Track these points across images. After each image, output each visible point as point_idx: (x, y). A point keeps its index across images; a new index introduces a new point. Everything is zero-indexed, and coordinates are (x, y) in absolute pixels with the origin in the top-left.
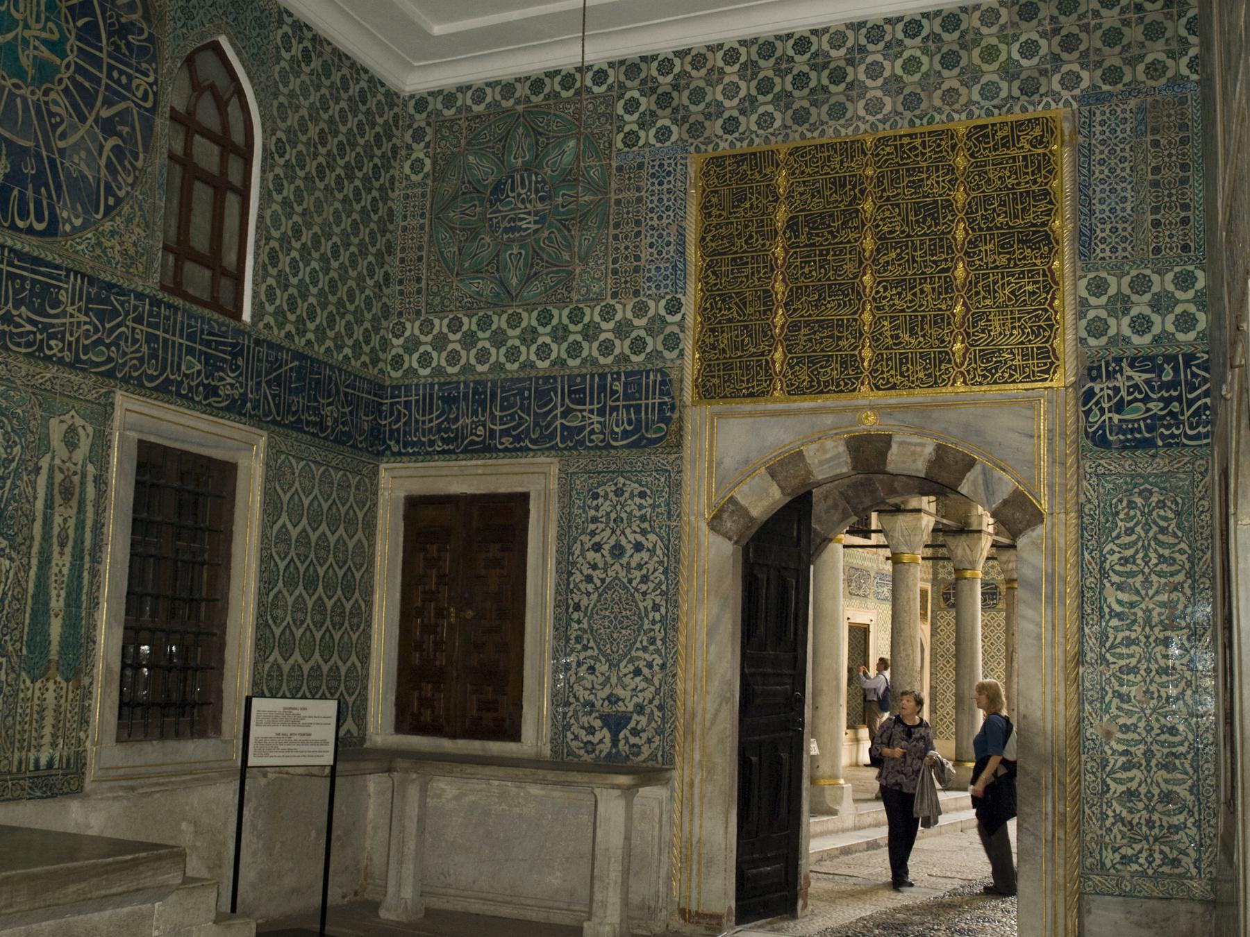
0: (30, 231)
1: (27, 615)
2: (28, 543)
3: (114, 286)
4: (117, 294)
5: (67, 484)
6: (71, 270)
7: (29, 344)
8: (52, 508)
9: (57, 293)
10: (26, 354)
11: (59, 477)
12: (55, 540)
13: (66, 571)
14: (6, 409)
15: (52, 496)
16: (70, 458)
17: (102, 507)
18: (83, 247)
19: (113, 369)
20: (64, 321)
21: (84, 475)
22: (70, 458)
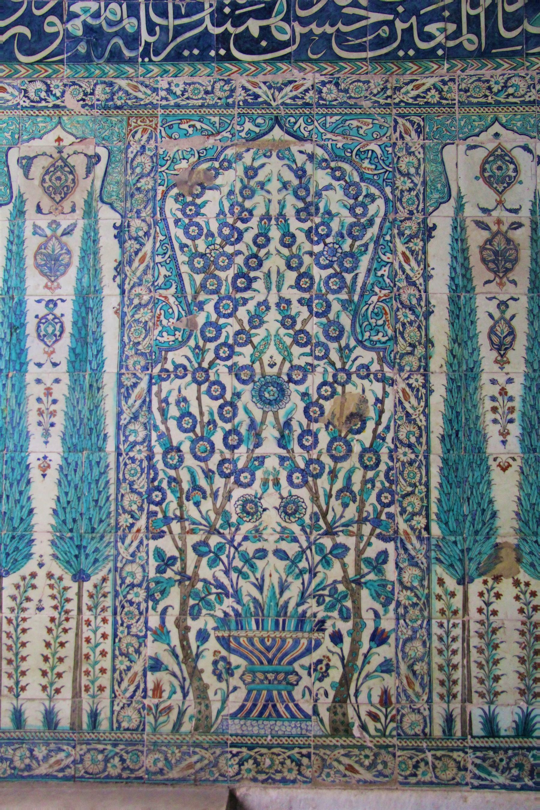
1: (434, 471)
2: (420, 351)
5: (499, 244)
7: (379, 43)
11: (476, 238)
12: (483, 340)
13: (516, 390)
14: (344, 148)
15: (467, 269)
16: (500, 203)
22: (500, 203)
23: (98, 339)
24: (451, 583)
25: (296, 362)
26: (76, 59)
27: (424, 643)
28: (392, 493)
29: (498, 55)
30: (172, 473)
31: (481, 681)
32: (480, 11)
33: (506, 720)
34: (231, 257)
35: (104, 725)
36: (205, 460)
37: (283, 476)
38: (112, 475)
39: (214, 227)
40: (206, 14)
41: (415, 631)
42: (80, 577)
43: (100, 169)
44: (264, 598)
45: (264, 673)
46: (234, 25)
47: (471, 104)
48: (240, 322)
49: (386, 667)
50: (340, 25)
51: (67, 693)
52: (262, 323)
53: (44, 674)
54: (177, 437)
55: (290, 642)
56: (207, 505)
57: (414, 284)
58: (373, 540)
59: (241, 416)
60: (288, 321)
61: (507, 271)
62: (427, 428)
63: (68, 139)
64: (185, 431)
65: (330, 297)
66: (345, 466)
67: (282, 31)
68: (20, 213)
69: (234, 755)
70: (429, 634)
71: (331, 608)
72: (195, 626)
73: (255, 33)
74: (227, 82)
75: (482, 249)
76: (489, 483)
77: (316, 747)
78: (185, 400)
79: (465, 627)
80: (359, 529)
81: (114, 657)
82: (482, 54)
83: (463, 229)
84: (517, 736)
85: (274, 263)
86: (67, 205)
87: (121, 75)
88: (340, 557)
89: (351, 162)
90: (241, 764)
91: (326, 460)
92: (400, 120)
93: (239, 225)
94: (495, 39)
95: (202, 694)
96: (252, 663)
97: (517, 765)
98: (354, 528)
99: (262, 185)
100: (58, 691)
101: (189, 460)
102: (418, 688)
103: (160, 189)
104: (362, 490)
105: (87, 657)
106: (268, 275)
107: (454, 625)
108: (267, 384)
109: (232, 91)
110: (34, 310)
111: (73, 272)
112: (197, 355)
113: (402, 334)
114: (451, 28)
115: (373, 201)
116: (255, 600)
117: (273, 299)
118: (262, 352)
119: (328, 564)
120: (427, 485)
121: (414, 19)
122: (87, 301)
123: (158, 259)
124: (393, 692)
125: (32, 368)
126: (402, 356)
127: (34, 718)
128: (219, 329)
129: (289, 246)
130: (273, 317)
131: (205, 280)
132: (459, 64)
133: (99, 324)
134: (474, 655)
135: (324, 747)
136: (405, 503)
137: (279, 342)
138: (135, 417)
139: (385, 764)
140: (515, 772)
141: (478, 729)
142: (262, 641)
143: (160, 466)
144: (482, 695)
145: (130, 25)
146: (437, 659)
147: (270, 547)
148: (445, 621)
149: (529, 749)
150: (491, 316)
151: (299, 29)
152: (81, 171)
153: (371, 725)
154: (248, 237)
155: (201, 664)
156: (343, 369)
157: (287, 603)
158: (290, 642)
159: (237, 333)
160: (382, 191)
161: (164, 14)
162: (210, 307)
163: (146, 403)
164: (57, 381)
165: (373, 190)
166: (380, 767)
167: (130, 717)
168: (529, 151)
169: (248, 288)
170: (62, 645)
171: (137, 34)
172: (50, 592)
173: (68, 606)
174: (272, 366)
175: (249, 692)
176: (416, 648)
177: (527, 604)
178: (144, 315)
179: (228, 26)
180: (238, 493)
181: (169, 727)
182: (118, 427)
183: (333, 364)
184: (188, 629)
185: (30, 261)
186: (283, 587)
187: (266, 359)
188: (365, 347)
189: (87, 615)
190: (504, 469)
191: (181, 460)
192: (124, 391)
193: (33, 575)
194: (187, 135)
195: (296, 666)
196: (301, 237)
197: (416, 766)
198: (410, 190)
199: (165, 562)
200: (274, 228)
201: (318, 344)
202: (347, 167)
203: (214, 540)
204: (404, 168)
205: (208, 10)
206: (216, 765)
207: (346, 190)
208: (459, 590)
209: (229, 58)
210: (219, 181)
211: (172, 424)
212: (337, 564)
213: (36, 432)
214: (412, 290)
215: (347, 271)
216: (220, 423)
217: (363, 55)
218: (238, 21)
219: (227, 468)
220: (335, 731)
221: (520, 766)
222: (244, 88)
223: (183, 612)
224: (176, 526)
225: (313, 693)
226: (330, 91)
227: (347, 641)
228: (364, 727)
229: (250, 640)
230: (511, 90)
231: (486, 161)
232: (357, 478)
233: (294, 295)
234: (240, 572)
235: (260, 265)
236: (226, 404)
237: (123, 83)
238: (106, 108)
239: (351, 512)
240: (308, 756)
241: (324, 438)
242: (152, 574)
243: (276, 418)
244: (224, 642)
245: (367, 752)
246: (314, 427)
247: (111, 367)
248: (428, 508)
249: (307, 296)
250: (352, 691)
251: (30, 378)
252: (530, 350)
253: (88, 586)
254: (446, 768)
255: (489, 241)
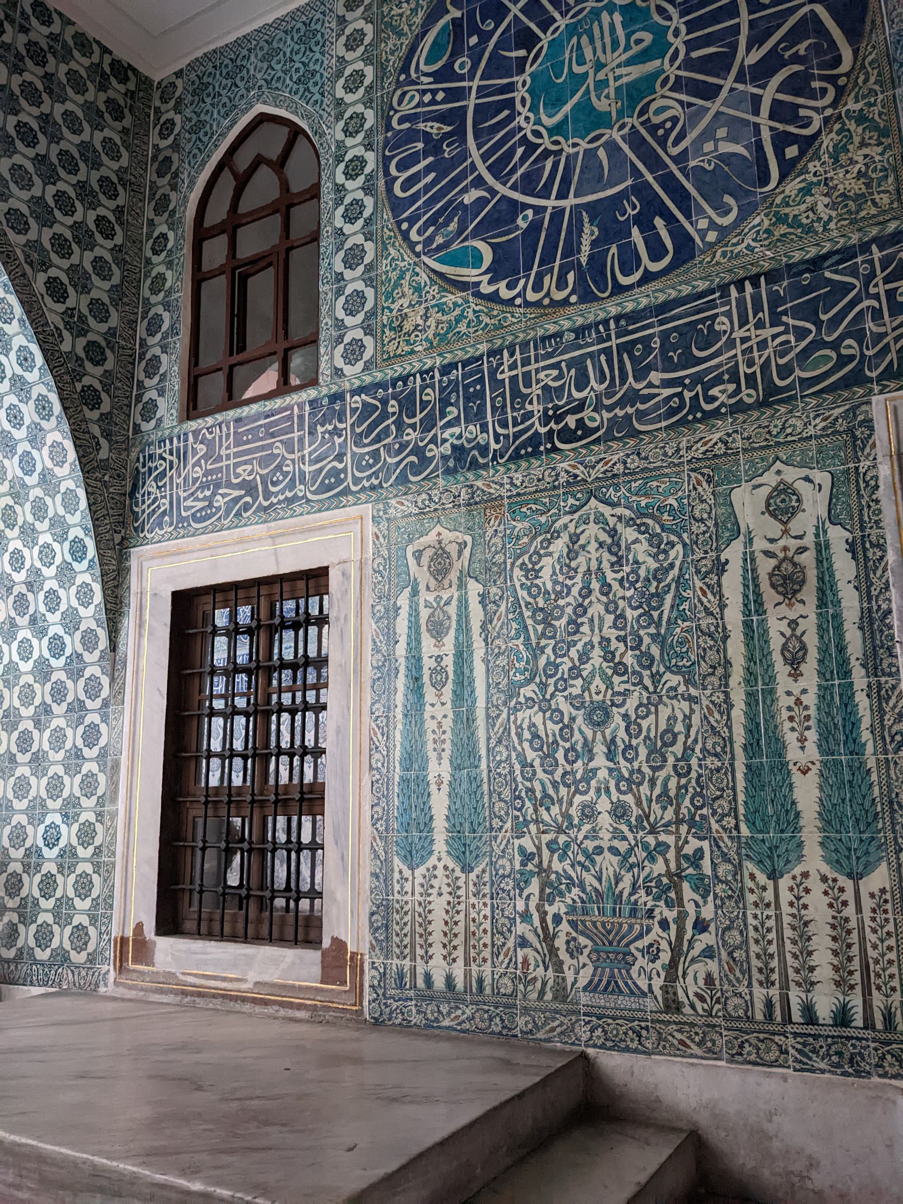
0: (648, 277)
1: (740, 776)
2: (720, 671)
3: (825, 257)
4: (838, 263)
5: (787, 568)
6: (729, 284)
7: (672, 412)
8: (760, 609)
9: (711, 328)
10: (667, 428)
11: (765, 566)
12: (777, 657)
13: (810, 700)
14: (647, 507)
15: (758, 595)
17: (878, 584)
18: (748, 241)
19: (859, 370)
20: (732, 353)
21: (822, 548)
22: (785, 532)
23: (472, 681)
24: (762, 878)
25: (616, 689)
26: (448, 472)
27: (741, 932)
28: (703, 797)
29: (774, 402)
30: (528, 784)
31: (797, 971)
32: (756, 368)
33: (824, 1009)
34: (562, 608)
35: (488, 991)
36: (551, 773)
37: (612, 784)
38: (485, 787)
39: (549, 586)
40: (535, 419)
41: (732, 922)
42: (467, 869)
43: (467, 552)
44: (603, 887)
45: (607, 952)
46: (557, 423)
47: (754, 449)
48: (572, 660)
49: (709, 953)
50: (638, 405)
51: (460, 962)
52: (589, 659)
53: (445, 946)
54: (530, 755)
55: (625, 927)
56: (555, 810)
57: (712, 614)
58: (690, 838)
59: (577, 736)
60: (609, 655)
61: (795, 592)
62: (731, 738)
63: (445, 533)
64: (536, 750)
65: (642, 632)
66: (662, 774)
67: (593, 419)
68: (415, 593)
69: (587, 1023)
70: (745, 925)
71: (657, 898)
72: (551, 910)
73: (572, 425)
74: (554, 469)
75: (771, 575)
76: (791, 785)
77: (652, 1021)
78: (534, 725)
79: (779, 918)
80: (677, 829)
81: (493, 935)
82: (762, 404)
83: (753, 560)
84: (835, 1025)
85: (596, 610)
86: (446, 582)
87: (478, 477)
88: (663, 854)
89: (652, 516)
90: (592, 1031)
91: (646, 770)
92: (693, 474)
93: (569, 582)
94: (771, 390)
95: (559, 966)
96: (596, 944)
97: (837, 1053)
98: (673, 828)
99: (583, 547)
100: (454, 960)
101: (540, 774)
102: (738, 974)
103: (509, 561)
104: (677, 795)
105: (474, 934)
106: (591, 620)
107: (768, 917)
108: (594, 710)
109: (557, 475)
110: (428, 663)
111: (452, 633)
112: (541, 690)
113: (703, 658)
114: (731, 387)
115: (673, 546)
116: (596, 890)
117: (596, 640)
118: (590, 683)
119: (653, 860)
120: (734, 789)
121: (699, 387)
122: (462, 656)
123: (511, 616)
124: (716, 976)
125: (428, 707)
126: (705, 677)
127: (439, 983)
128: (557, 667)
129: (606, 594)
130: (597, 653)
131: (545, 629)
132: (741, 417)
133: (472, 671)
134: (789, 946)
135: (658, 1021)
136: (716, 806)
137: (603, 673)
138: (500, 741)
139: (713, 1042)
140: (835, 1059)
141: (796, 1016)
142: (603, 924)
143: (519, 779)
144: (799, 984)
145: (482, 439)
146: (754, 948)
147: (605, 844)
148: (759, 912)
149: (848, 1038)
150: (783, 634)
151: (606, 415)
152: (454, 555)
153: (699, 1005)
154: (575, 591)
155: (557, 943)
156: (655, 692)
157: (621, 892)
158: (625, 927)
159: (570, 669)
160: (680, 537)
161: (505, 425)
162: (549, 651)
163: (507, 730)
164: (445, 716)
165: (673, 538)
166: (709, 1044)
167: (507, 985)
168: (811, 481)
169: (577, 631)
170: (456, 923)
171: (488, 443)
172: (446, 881)
173: (459, 893)
174: (598, 693)
175: (596, 969)
176: (734, 937)
177: (836, 899)
178: (502, 661)
179: (552, 424)
180: (578, 799)
181: (535, 995)
182: (488, 750)
183: (646, 688)
184: (546, 913)
185: (423, 628)
186: (618, 879)
187: (593, 688)
188: (672, 672)
189: (473, 900)
190: (804, 773)
191: (534, 773)
192: (491, 720)
193: (435, 867)
194: (526, 516)
195: (632, 948)
196: (615, 586)
197: (741, 1046)
198: (704, 533)
199: (527, 858)
200: (594, 581)
201: (634, 673)
202: (650, 522)
203: (562, 839)
204: (697, 515)
205: (537, 415)
206: (572, 1031)
207: (650, 541)
208: (770, 884)
209: (555, 449)
210: (551, 549)
211: (526, 745)
212: (660, 860)
213: (432, 755)
214: (710, 620)
215: (655, 609)
216: (561, 743)
217: (658, 426)
218: (559, 419)
219: (569, 779)
220: (667, 1009)
221: (839, 1054)
222: (567, 472)
223: (541, 898)
224: (533, 828)
225: (648, 975)
226: (633, 461)
227: (673, 927)
228: (693, 1006)
229: (594, 924)
230: (789, 431)
231: (770, 497)
232: (673, 784)
233: (612, 634)
234: (583, 866)
235: (585, 612)
236: (565, 726)
237: (479, 483)
238: (469, 505)
239: (669, 814)
240: (647, 1028)
241: (643, 752)
242: (517, 866)
243: (604, 737)
244: (573, 924)
245: (697, 1029)
246: (634, 742)
247: (481, 703)
248: (736, 810)
249: (622, 633)
250: (680, 973)
251: (427, 716)
252: (821, 662)
253: (472, 876)
254: (768, 1050)
255: (778, 567)
